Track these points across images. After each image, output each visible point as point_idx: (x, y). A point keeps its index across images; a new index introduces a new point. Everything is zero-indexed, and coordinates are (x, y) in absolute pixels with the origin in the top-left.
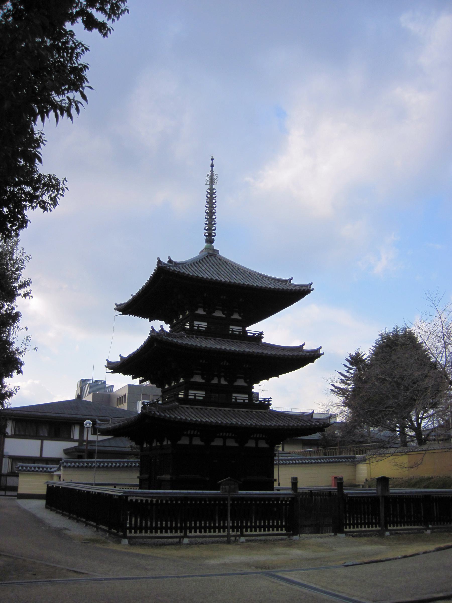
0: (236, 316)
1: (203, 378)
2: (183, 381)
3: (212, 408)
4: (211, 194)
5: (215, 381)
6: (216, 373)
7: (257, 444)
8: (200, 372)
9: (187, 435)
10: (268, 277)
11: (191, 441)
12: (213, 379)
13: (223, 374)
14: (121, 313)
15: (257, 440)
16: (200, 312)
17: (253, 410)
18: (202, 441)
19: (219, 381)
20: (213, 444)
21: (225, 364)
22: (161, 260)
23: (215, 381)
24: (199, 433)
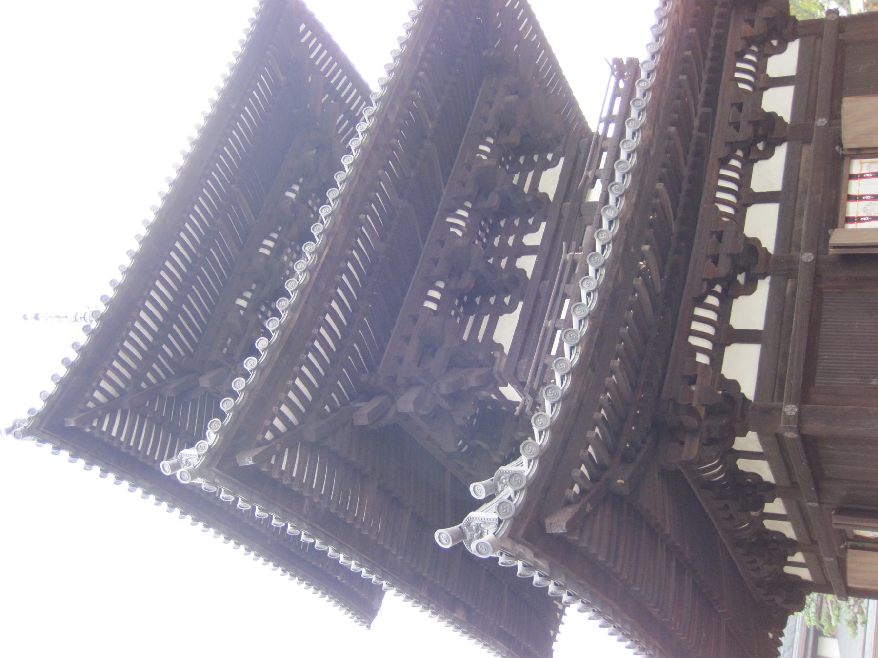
1: (510, 309)
2: (509, 385)
8: (486, 319)
9: (717, 357)
12: (523, 271)
13: (511, 241)
14: (379, 611)
19: (531, 251)
21: (461, 223)
22: (10, 425)
23: (527, 264)
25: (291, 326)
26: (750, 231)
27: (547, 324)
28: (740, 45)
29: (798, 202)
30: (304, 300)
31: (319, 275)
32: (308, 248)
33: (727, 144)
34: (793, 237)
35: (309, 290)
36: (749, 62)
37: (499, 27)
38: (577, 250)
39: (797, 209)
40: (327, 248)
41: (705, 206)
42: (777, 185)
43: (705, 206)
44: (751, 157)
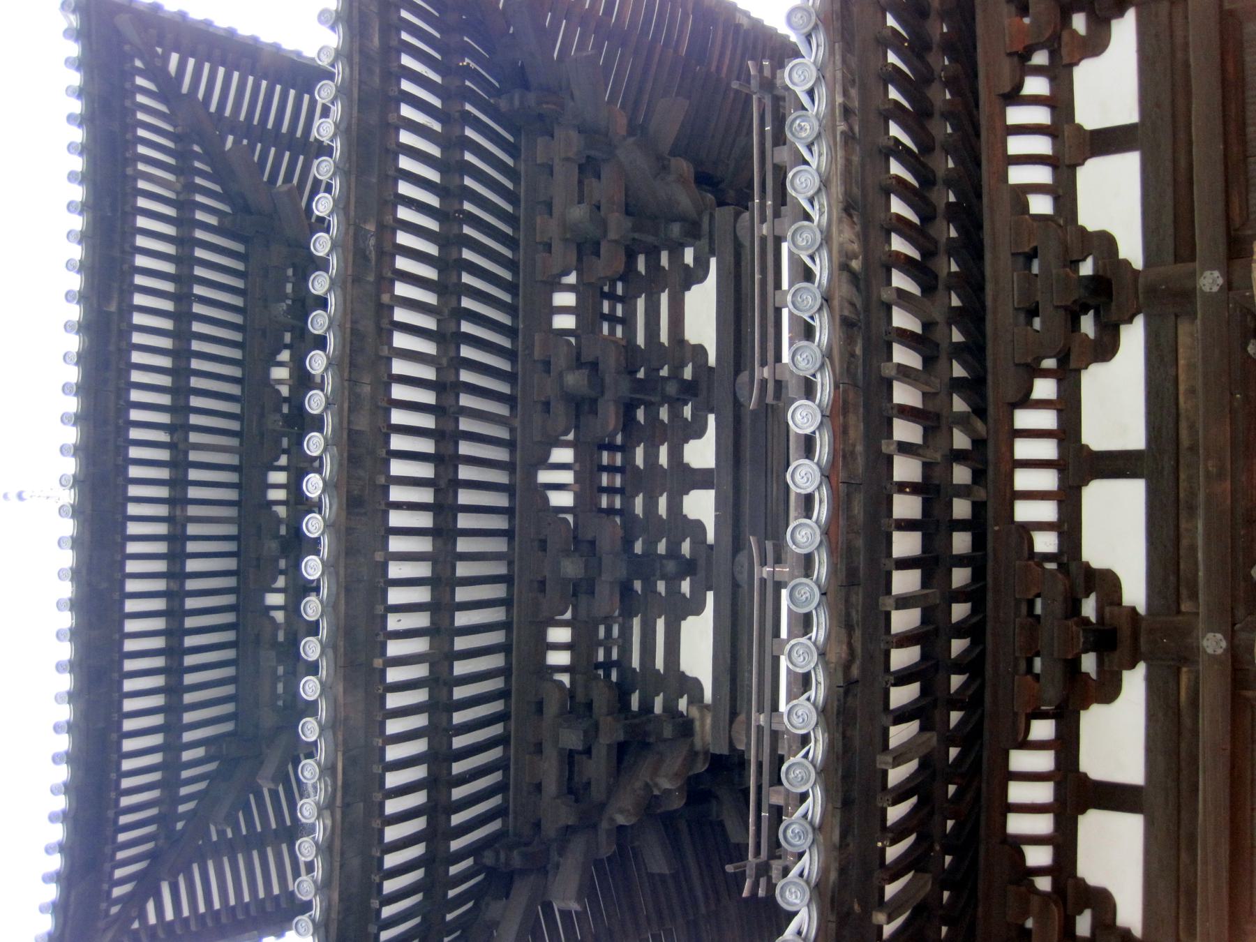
18: (1108, 690)
19: (702, 479)
24: (1042, 729)
25: (334, 915)
27: (758, 720)
28: (1006, 67)
29: (1182, 476)
30: (337, 865)
31: (346, 806)
32: (309, 771)
33: (1010, 55)
34: (1182, 566)
35: (337, 843)
36: (1035, 100)
37: (511, 31)
38: (778, 561)
39: (1182, 495)
40: (340, 755)
41: (996, 528)
42: (1133, 437)
43: (996, 528)
44: (1073, 365)
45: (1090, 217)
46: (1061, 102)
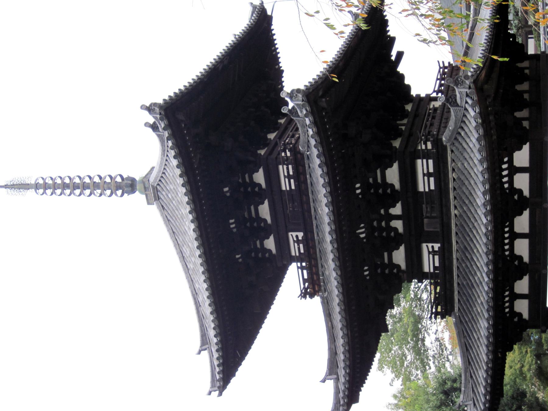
0: (259, 177)
3: (454, 256)
4: (45, 186)
5: (398, 225)
6: (383, 224)
7: (522, 170)
10: (163, 148)
11: (522, 296)
12: (396, 229)
15: (514, 170)
16: (270, 244)
17: (450, 176)
19: (397, 217)
20: (526, 259)
26: (517, 252)
42: (526, 230)
45: (517, 185)
46: (511, 161)
